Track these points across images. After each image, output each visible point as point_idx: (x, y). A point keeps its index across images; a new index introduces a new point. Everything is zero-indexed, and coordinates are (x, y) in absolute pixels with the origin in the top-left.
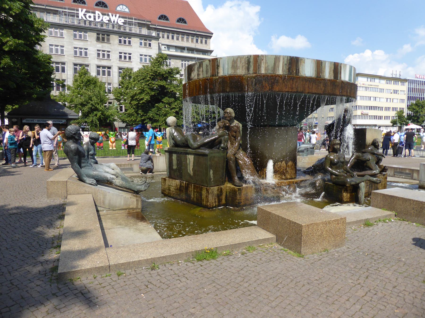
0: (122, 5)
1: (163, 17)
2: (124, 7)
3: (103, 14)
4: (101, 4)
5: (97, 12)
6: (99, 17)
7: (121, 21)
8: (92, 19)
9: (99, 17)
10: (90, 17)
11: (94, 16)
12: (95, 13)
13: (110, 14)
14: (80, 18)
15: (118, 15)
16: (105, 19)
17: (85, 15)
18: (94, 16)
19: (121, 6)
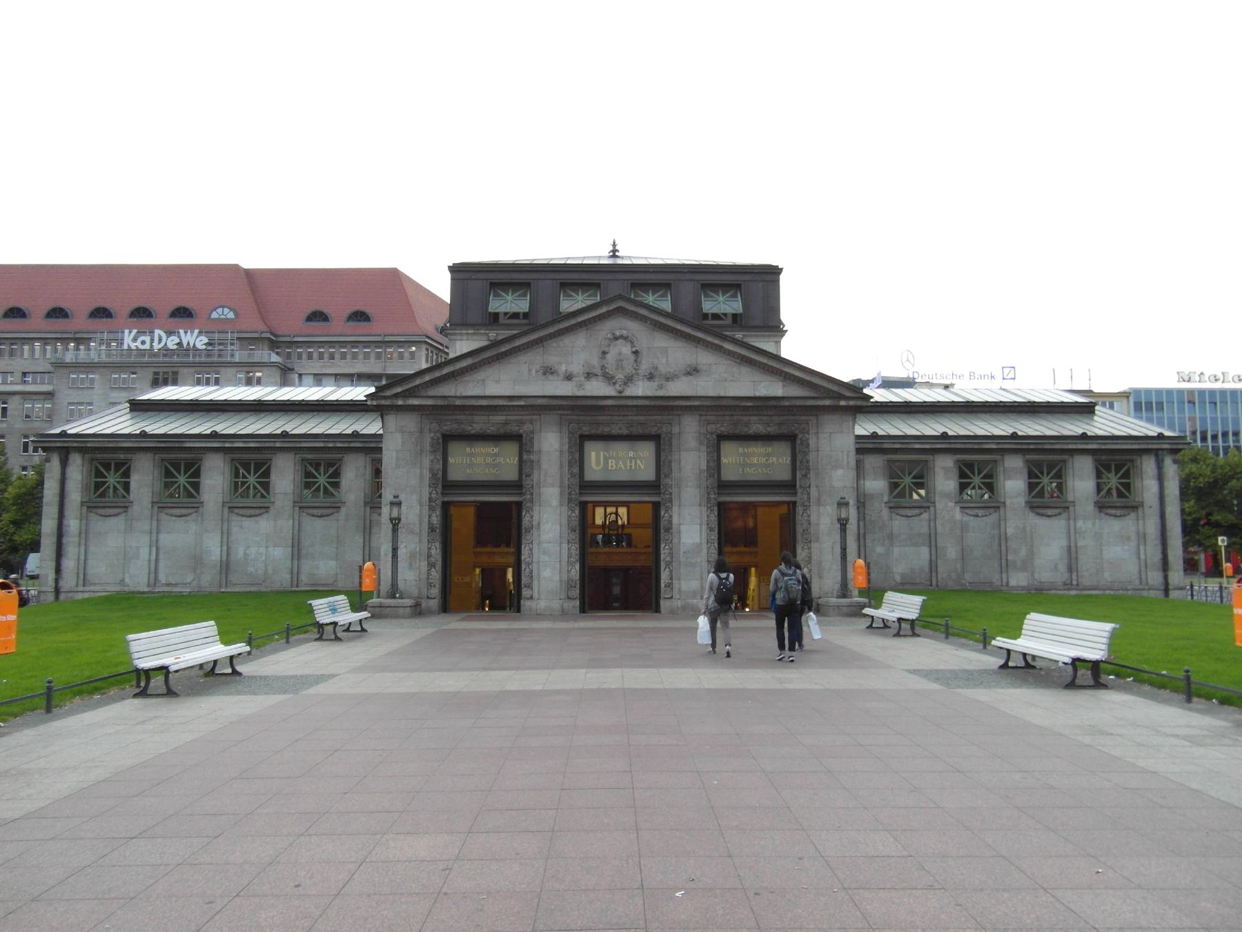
0: (223, 307)
1: (318, 316)
2: (226, 310)
3: (169, 333)
4: (182, 313)
5: (157, 332)
6: (160, 340)
7: (202, 342)
8: (147, 346)
9: (160, 340)
10: (143, 343)
11: (152, 340)
12: (152, 332)
13: (182, 331)
14: (125, 347)
15: (196, 331)
16: (172, 343)
17: (135, 340)
18: (152, 340)
19: (220, 310)
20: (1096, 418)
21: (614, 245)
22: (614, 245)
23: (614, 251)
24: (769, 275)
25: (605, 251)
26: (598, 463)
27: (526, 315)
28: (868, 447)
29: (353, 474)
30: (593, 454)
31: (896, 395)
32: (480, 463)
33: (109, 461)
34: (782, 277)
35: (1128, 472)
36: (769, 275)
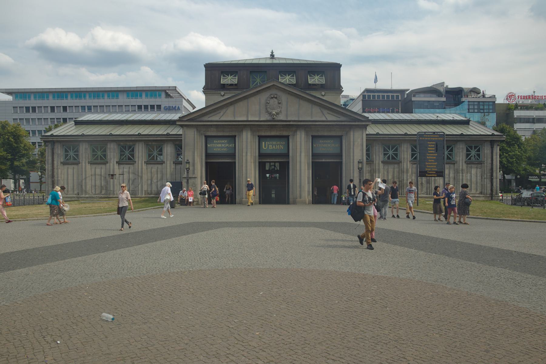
20: (470, 127)
21: (272, 53)
22: (272, 53)
23: (272, 56)
24: (337, 67)
25: (268, 55)
26: (265, 147)
27: (236, 85)
28: (372, 140)
29: (169, 150)
30: (263, 143)
31: (389, 116)
32: (219, 146)
33: (70, 144)
34: (341, 68)
35: (479, 149)
36: (337, 67)
